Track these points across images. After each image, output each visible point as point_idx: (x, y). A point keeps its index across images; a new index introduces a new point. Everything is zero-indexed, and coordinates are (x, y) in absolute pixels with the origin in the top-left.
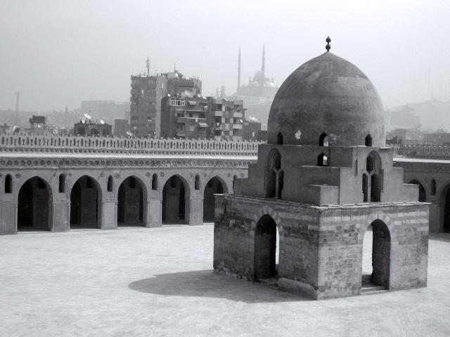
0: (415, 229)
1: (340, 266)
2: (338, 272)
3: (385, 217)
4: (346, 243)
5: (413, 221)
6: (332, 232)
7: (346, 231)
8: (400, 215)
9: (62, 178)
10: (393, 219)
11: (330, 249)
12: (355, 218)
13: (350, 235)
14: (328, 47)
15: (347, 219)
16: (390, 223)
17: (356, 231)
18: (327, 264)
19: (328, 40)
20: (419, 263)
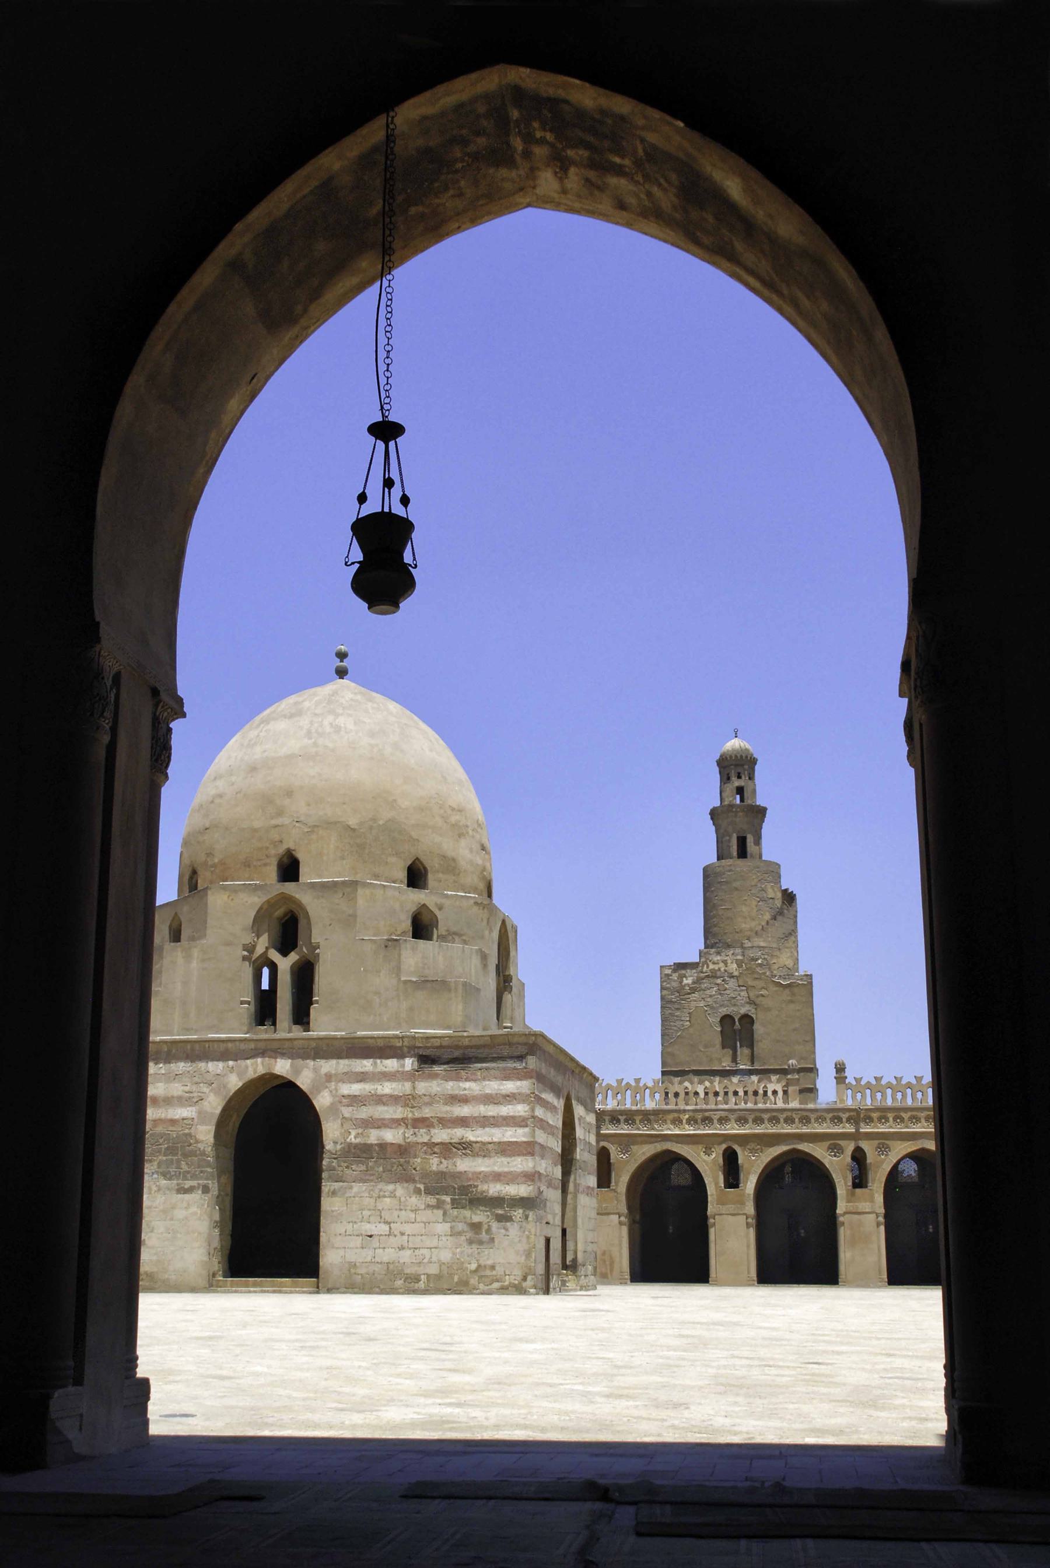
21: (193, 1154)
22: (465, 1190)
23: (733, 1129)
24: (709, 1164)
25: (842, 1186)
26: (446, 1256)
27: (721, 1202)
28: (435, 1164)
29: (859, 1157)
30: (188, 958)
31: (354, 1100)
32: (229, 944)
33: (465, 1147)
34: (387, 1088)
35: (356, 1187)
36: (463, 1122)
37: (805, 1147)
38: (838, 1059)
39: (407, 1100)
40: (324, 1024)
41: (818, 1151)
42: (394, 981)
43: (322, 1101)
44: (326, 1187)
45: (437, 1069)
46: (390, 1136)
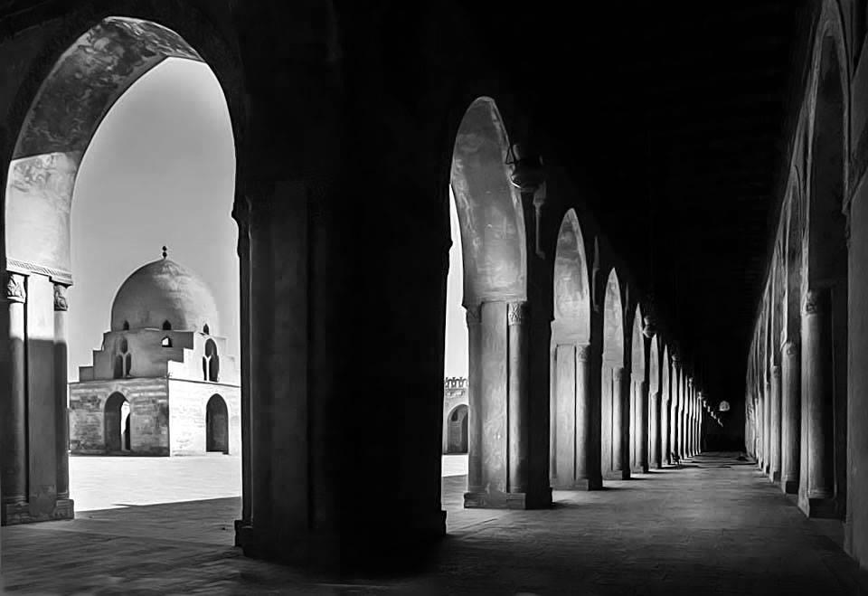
1: (87, 429)
2: (85, 434)
4: (90, 411)
5: (151, 394)
6: (78, 401)
7: (89, 401)
8: (139, 388)
10: (130, 392)
12: (96, 390)
14: (165, 255)
15: (90, 391)
19: (164, 249)
20: (160, 432)
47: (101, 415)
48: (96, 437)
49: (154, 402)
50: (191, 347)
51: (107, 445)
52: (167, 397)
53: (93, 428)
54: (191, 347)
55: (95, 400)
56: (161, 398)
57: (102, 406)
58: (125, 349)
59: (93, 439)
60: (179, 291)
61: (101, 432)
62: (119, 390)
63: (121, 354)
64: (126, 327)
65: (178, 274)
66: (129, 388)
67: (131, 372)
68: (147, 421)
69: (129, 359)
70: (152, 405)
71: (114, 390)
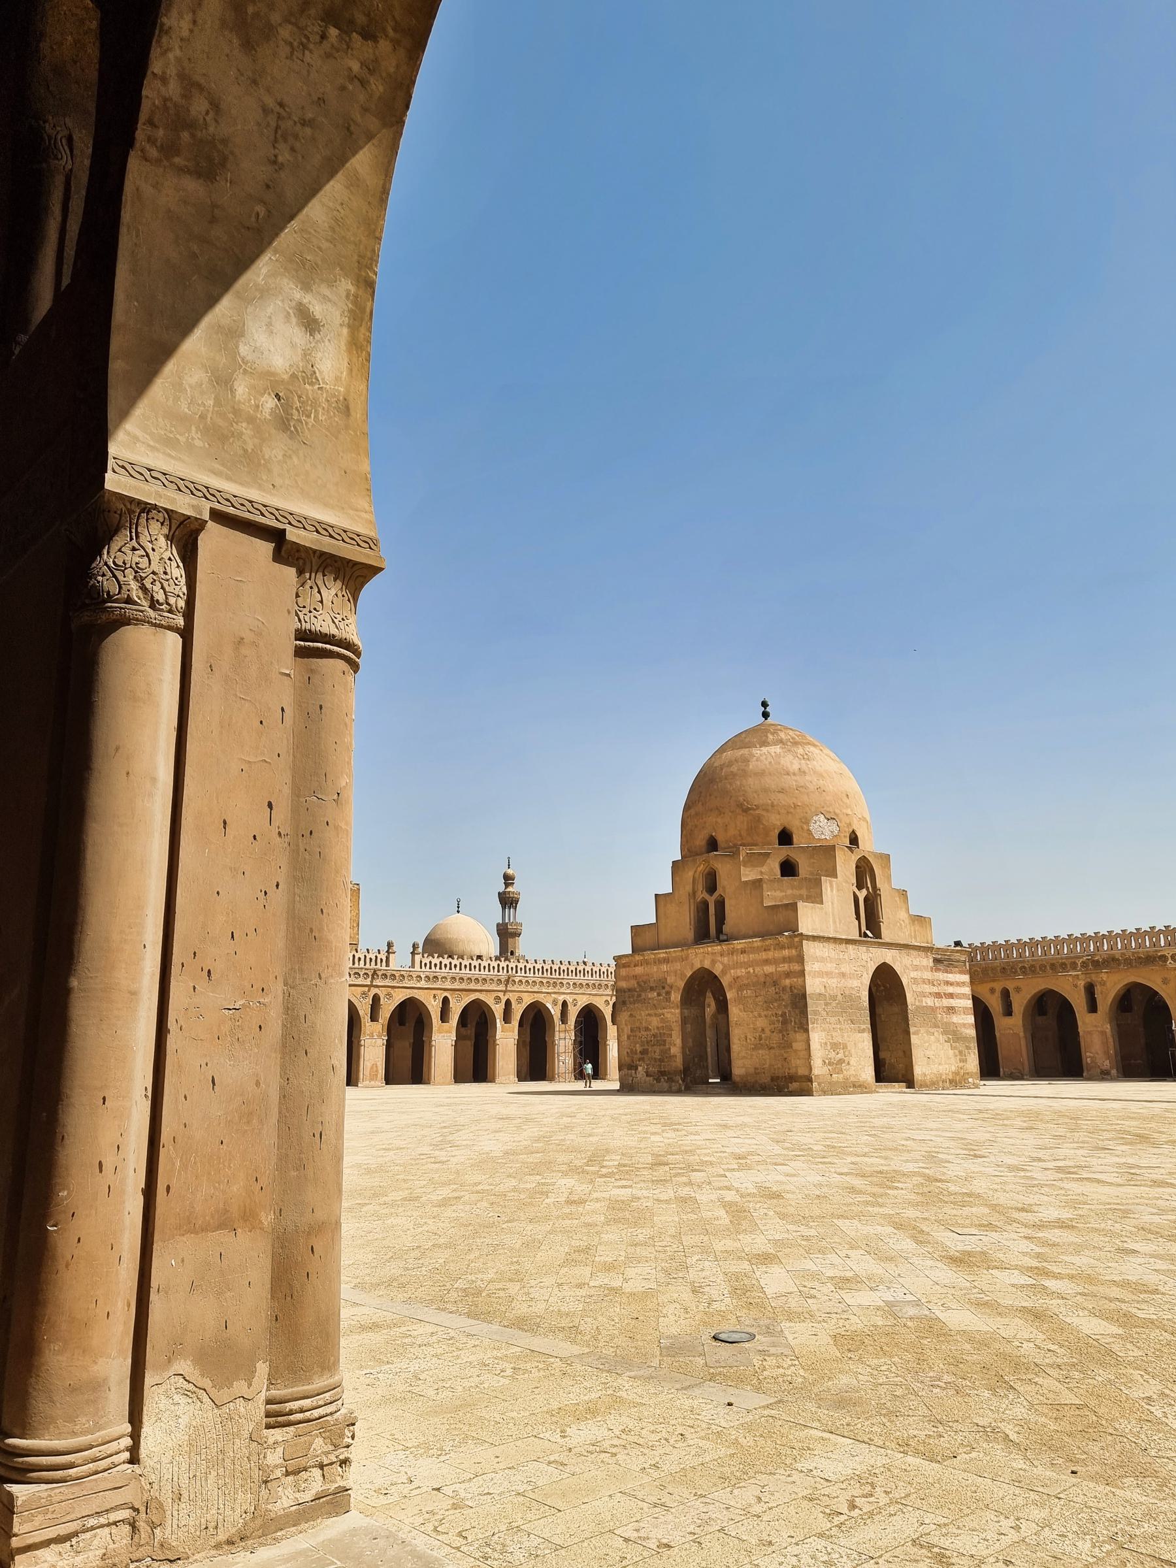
0: (775, 984)
3: (713, 962)
5: (769, 969)
7: (652, 989)
8: (743, 958)
9: (1090, 990)
11: (631, 1015)
12: (664, 967)
13: (659, 995)
14: (766, 715)
16: (724, 972)
17: (667, 988)
18: (629, 1037)
19: (764, 704)
21: (859, 1009)
22: (954, 1033)
23: (448, 985)
24: (434, 1007)
25: (499, 1023)
26: (953, 1068)
27: (440, 1032)
28: (946, 1018)
29: (508, 1003)
30: (831, 886)
31: (915, 981)
32: (847, 882)
33: (951, 1010)
34: (928, 975)
35: (922, 1030)
36: (951, 996)
37: (482, 997)
38: (390, 939)
39: (931, 983)
40: (887, 935)
41: (489, 1000)
42: (906, 916)
43: (905, 981)
44: (912, 1030)
45: (941, 967)
46: (929, 1002)
47: (673, 1014)
48: (666, 1056)
49: (775, 984)
50: (833, 874)
51: (686, 1071)
52: (802, 973)
53: (660, 1039)
54: (833, 874)
55: (662, 986)
56: (788, 975)
57: (676, 997)
58: (712, 887)
59: (661, 1060)
60: (802, 772)
61: (676, 1049)
62: (707, 964)
63: (706, 896)
64: (713, 845)
65: (796, 743)
66: (725, 960)
67: (726, 928)
68: (761, 1023)
69: (721, 905)
70: (772, 990)
71: (698, 966)
